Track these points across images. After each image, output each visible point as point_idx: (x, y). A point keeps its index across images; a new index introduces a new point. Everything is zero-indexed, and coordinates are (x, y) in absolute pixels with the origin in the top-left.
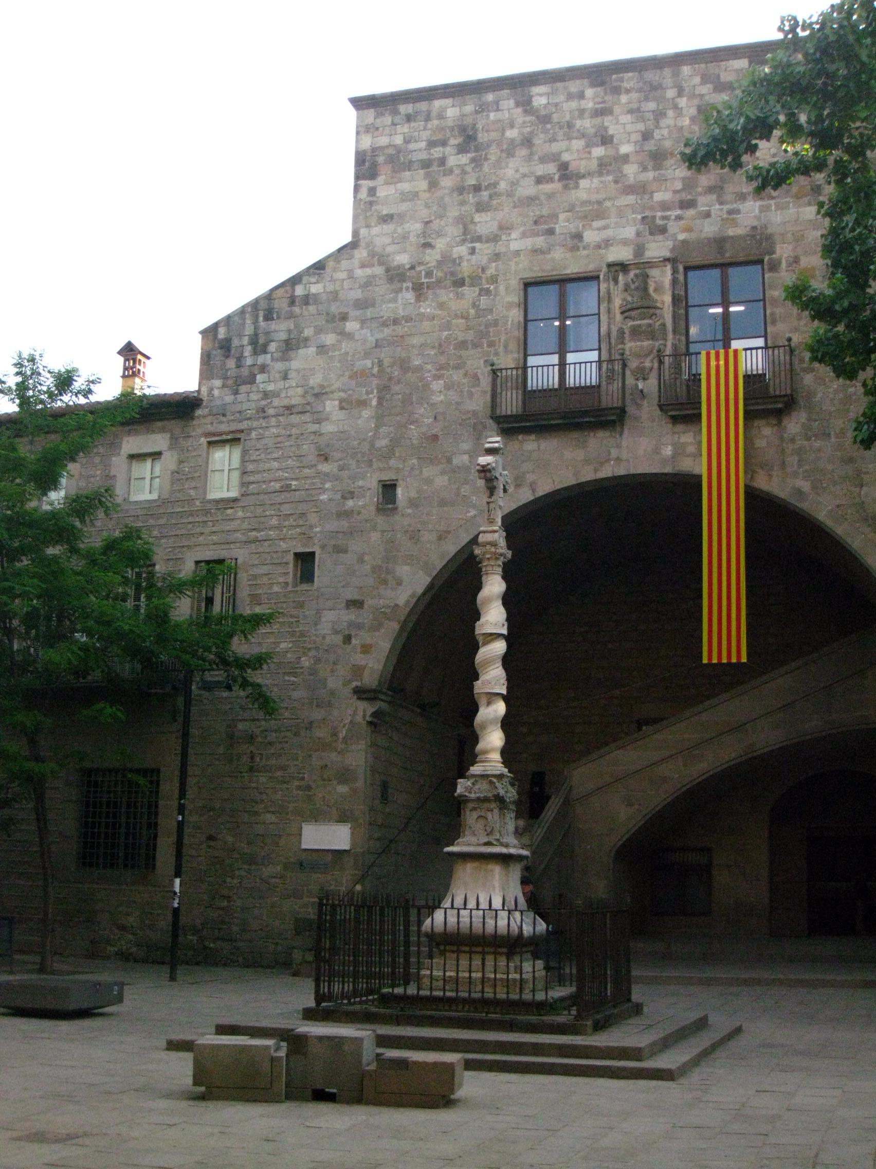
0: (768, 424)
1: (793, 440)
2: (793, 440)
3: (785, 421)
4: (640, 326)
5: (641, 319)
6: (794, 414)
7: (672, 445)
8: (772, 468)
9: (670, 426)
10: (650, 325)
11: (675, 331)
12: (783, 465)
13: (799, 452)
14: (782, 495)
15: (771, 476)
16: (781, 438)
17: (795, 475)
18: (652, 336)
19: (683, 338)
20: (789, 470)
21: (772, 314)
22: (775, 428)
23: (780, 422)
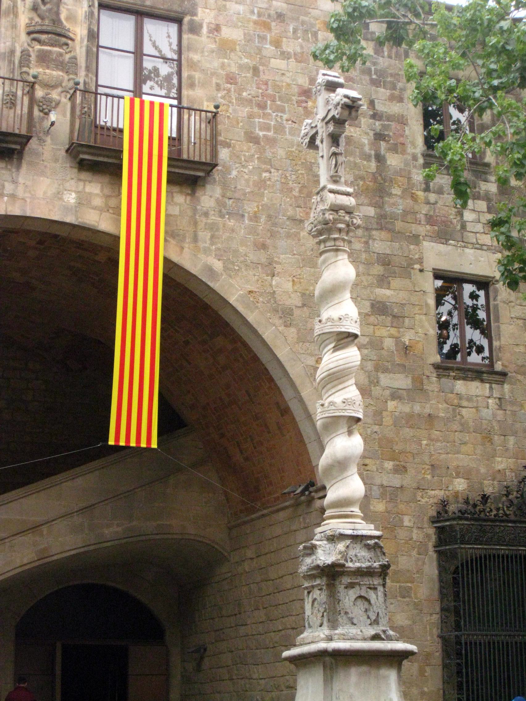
0: (181, 192)
1: (206, 214)
2: (206, 214)
3: (199, 193)
4: (50, 52)
5: (52, 45)
6: (208, 187)
7: (77, 192)
8: (183, 240)
9: (76, 170)
10: (61, 55)
11: (88, 69)
12: (195, 239)
13: (212, 227)
14: (194, 270)
15: (182, 248)
16: (195, 210)
17: (206, 251)
18: (61, 65)
19: (94, 78)
20: (201, 245)
21: (190, 77)
22: (189, 198)
23: (193, 193)
